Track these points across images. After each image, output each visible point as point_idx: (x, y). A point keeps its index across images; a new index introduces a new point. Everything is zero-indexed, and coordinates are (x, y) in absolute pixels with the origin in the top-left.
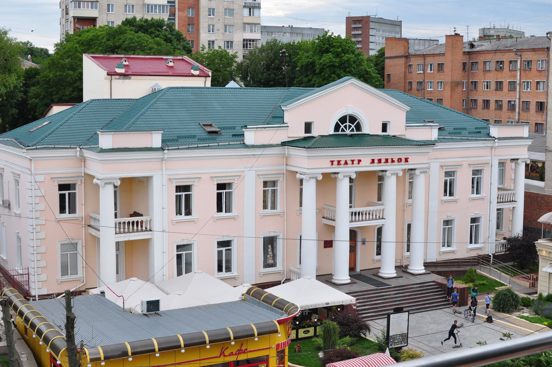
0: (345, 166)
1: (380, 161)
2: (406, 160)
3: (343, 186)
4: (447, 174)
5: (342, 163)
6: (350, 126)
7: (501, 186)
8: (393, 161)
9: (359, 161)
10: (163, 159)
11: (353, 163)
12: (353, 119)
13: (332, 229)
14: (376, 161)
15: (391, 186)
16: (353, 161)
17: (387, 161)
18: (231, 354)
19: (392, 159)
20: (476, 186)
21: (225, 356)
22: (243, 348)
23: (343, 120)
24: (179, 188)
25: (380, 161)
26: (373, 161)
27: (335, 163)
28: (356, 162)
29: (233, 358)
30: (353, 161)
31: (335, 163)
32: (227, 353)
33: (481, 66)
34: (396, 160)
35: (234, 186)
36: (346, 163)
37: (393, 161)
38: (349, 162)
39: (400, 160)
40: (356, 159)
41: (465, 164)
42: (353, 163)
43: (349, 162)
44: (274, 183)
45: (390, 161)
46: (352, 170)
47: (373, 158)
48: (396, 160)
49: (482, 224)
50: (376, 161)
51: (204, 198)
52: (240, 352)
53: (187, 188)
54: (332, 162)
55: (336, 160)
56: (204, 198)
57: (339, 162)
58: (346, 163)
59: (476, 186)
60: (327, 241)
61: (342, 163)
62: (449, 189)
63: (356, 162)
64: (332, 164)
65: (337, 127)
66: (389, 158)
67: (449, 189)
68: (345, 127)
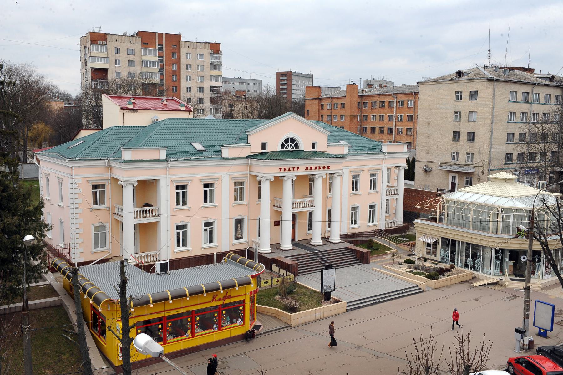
2: (328, 167)
3: (288, 185)
4: (354, 177)
5: (287, 169)
6: (291, 145)
7: (388, 184)
8: (320, 168)
9: (298, 168)
10: (167, 167)
12: (293, 140)
13: (280, 213)
14: (309, 168)
15: (318, 185)
16: (294, 168)
17: (316, 168)
18: (220, 299)
20: (373, 185)
21: (216, 301)
22: (228, 295)
23: (286, 141)
24: (178, 187)
25: (311, 168)
26: (307, 168)
27: (282, 170)
28: (296, 169)
29: (221, 303)
30: (294, 168)
31: (282, 170)
32: (217, 298)
33: (369, 105)
34: (322, 168)
35: (215, 186)
36: (289, 170)
38: (292, 169)
39: (324, 168)
40: (296, 167)
41: (366, 170)
43: (292, 169)
44: (241, 183)
45: (318, 168)
46: (293, 175)
48: (322, 168)
49: (377, 209)
50: (309, 168)
51: (195, 193)
52: (226, 297)
53: (183, 187)
54: (280, 169)
55: (283, 167)
56: (195, 193)
57: (285, 169)
58: (289, 170)
59: (373, 185)
61: (287, 169)
62: (355, 186)
63: (296, 169)
65: (283, 146)
67: (355, 186)
68: (288, 145)
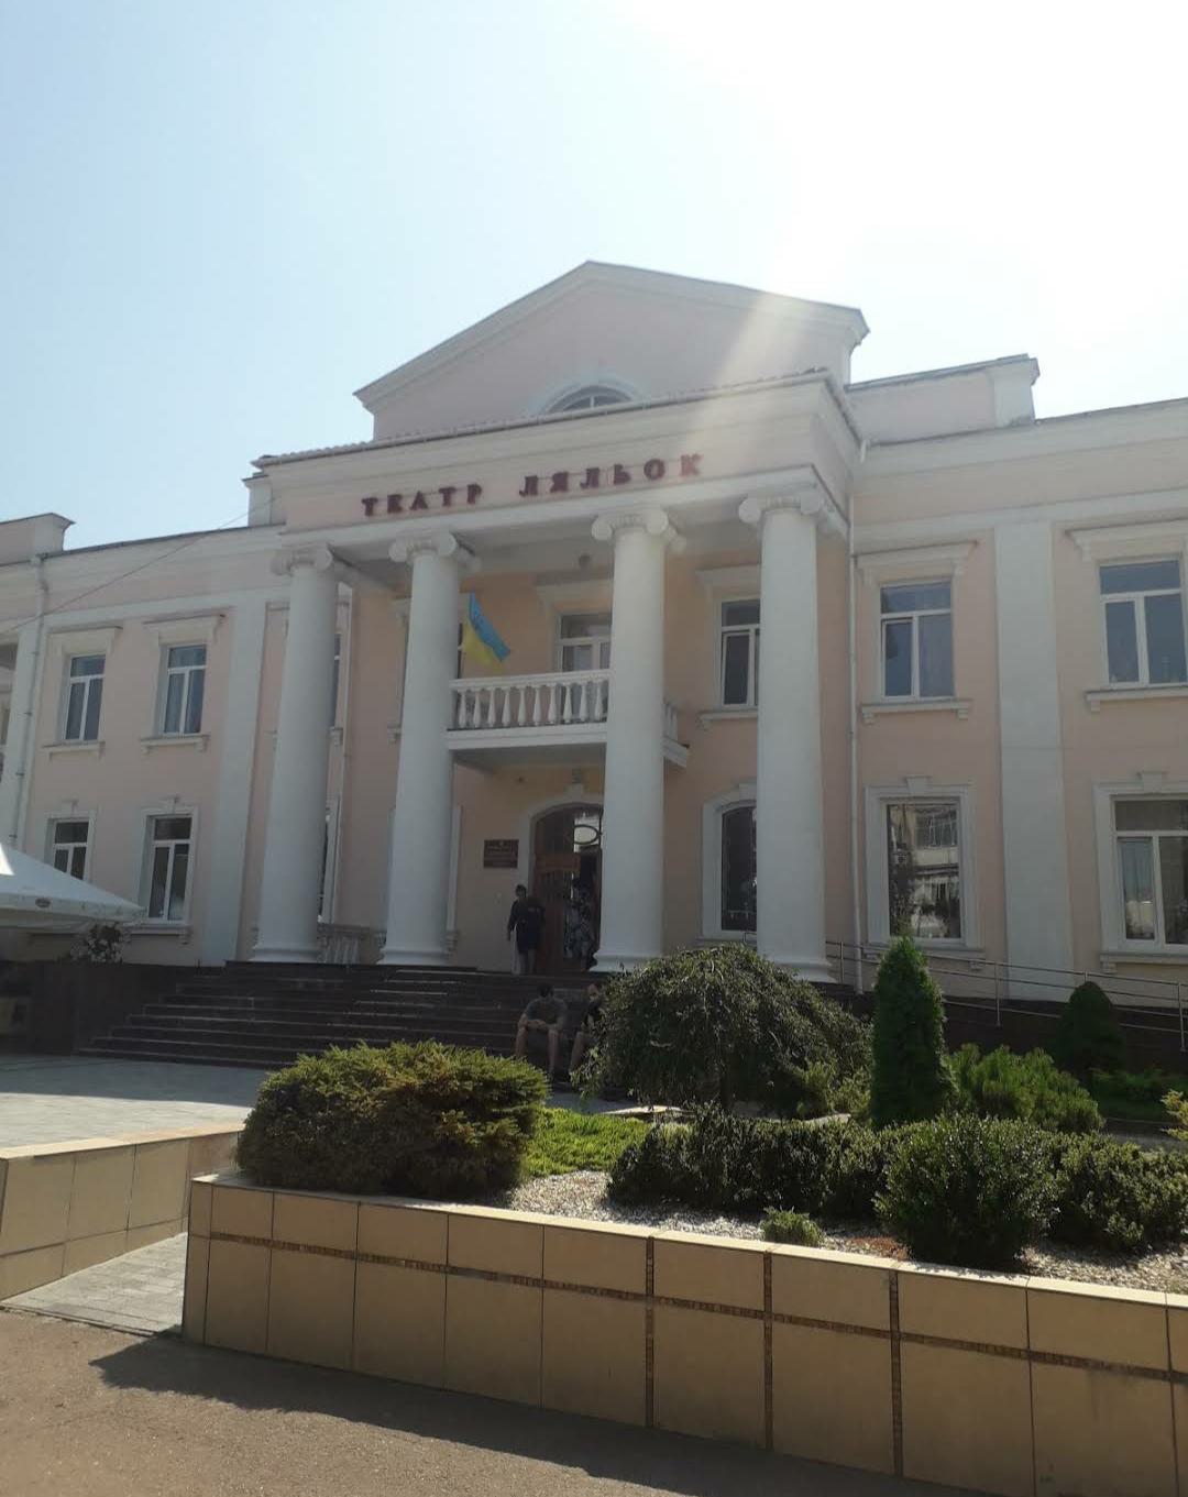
1: (561, 482)
3: (431, 596)
5: (407, 503)
8: (621, 476)
9: (474, 491)
11: (447, 502)
14: (545, 485)
19: (618, 468)
26: (531, 486)
27: (382, 507)
28: (460, 498)
31: (382, 507)
34: (637, 474)
37: (621, 476)
40: (461, 480)
42: (447, 502)
43: (436, 500)
45: (607, 477)
47: (530, 472)
48: (637, 474)
50: (545, 485)
54: (370, 504)
60: (496, 842)
61: (407, 503)
63: (460, 498)
64: (369, 512)
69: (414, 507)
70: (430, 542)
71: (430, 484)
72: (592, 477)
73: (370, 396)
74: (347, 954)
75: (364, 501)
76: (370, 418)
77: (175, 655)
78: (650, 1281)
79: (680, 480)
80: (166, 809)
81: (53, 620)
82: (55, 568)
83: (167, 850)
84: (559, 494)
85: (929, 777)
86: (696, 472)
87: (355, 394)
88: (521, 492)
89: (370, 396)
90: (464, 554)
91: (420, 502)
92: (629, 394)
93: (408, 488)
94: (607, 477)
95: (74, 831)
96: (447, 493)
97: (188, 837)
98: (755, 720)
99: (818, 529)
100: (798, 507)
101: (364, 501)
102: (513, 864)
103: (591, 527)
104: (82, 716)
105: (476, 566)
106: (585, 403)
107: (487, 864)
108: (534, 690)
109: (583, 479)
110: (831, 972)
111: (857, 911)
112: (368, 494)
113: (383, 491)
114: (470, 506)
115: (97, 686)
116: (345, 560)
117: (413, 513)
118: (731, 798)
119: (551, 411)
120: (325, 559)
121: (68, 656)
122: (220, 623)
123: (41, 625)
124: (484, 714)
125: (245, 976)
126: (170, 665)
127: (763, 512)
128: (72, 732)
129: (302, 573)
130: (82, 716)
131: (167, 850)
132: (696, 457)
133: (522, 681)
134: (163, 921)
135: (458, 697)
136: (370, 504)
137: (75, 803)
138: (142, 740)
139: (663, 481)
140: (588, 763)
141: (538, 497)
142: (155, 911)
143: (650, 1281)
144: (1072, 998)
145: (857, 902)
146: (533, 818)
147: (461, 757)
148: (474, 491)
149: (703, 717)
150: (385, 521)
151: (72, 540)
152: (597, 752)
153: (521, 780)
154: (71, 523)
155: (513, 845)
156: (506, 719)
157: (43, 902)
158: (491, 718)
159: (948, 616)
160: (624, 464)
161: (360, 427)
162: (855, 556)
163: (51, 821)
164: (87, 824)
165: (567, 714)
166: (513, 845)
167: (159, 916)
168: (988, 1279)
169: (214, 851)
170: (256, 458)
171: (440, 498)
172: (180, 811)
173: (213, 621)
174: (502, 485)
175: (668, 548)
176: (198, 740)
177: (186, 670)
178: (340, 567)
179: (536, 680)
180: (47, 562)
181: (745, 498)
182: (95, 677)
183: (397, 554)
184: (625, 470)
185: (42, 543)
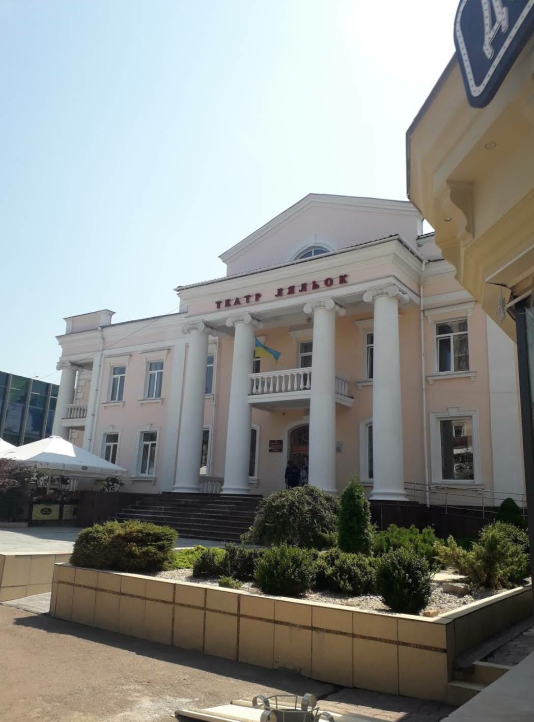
0: (238, 306)
1: (291, 290)
2: (343, 279)
3: (242, 340)
5: (233, 303)
8: (315, 286)
9: (258, 296)
11: (248, 301)
26: (280, 292)
27: (223, 304)
28: (253, 299)
31: (223, 304)
34: (322, 284)
37: (315, 286)
39: (329, 282)
40: (253, 292)
42: (248, 301)
43: (243, 301)
45: (310, 287)
48: (322, 284)
50: (285, 292)
54: (219, 303)
61: (233, 303)
63: (253, 299)
64: (219, 307)
66: (309, 280)
69: (235, 304)
70: (240, 318)
71: (241, 294)
72: (304, 287)
73: (225, 257)
74: (207, 489)
75: (216, 303)
76: (225, 266)
77: (152, 366)
78: (174, 598)
79: (339, 285)
80: (147, 429)
81: (106, 353)
82: (107, 331)
83: (148, 445)
84: (291, 295)
85: (458, 408)
86: (345, 282)
87: (219, 257)
88: (276, 295)
89: (225, 257)
90: (255, 322)
91: (237, 302)
92: (330, 249)
93: (233, 296)
94: (310, 287)
95: (113, 438)
96: (248, 298)
97: (156, 440)
98: (372, 386)
99: (399, 302)
100: (387, 294)
101: (216, 303)
102: (281, 450)
103: (303, 308)
104: (117, 391)
105: (261, 326)
106: (309, 254)
107: (271, 451)
108: (288, 376)
109: (300, 288)
110: (406, 496)
111: (427, 469)
112: (218, 300)
113: (223, 298)
114: (256, 302)
115: (123, 378)
116: (211, 327)
117: (235, 306)
118: (368, 421)
119: (295, 259)
120: (202, 327)
121: (112, 367)
122: (168, 353)
123: (102, 355)
124: (269, 387)
125: (169, 498)
126: (150, 370)
127: (373, 297)
128: (113, 398)
129: (194, 332)
130: (117, 391)
131: (148, 445)
132: (346, 276)
133: (283, 373)
134: (146, 475)
135: (253, 381)
136: (219, 304)
137: (113, 427)
138: (139, 401)
139: (331, 287)
140: (304, 406)
141: (283, 297)
142: (143, 471)
143: (174, 598)
144: (501, 505)
145: (426, 464)
146: (289, 430)
147: (254, 405)
148: (258, 296)
149: (358, 385)
150: (224, 310)
151: (115, 320)
152: (306, 403)
153: (284, 414)
154: (115, 313)
155: (281, 442)
156: (277, 389)
157: (85, 468)
158: (271, 389)
159: (467, 334)
160: (316, 281)
161: (220, 271)
162: (423, 311)
163: (105, 434)
164: (118, 435)
165: (302, 386)
166: (281, 442)
167: (145, 473)
168: (267, 597)
169: (164, 446)
170: (176, 287)
171: (245, 299)
172: (153, 429)
173: (166, 352)
174: (269, 293)
175: (337, 313)
176: (160, 401)
177: (156, 372)
178: (209, 330)
179: (289, 372)
180: (104, 329)
181: (366, 291)
182: (121, 375)
183: (229, 324)
184: (317, 283)
185: (103, 321)
